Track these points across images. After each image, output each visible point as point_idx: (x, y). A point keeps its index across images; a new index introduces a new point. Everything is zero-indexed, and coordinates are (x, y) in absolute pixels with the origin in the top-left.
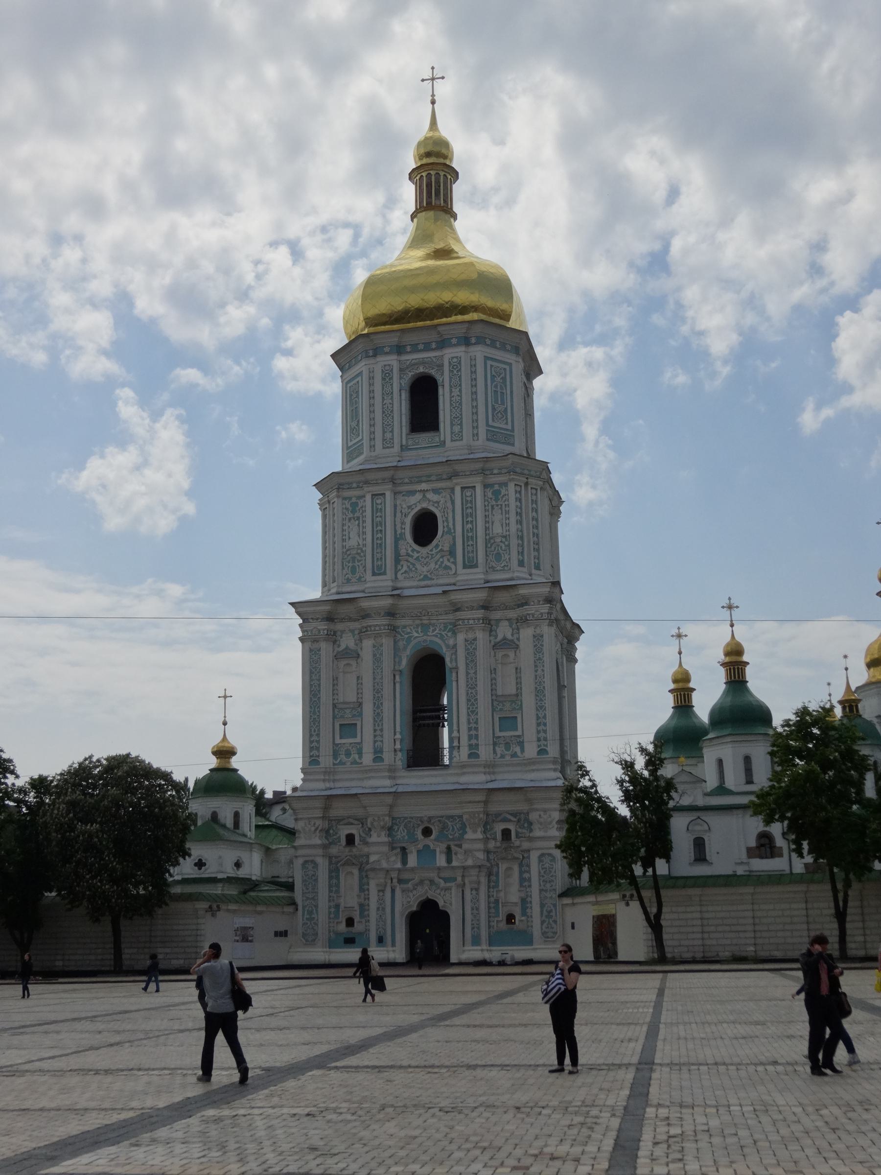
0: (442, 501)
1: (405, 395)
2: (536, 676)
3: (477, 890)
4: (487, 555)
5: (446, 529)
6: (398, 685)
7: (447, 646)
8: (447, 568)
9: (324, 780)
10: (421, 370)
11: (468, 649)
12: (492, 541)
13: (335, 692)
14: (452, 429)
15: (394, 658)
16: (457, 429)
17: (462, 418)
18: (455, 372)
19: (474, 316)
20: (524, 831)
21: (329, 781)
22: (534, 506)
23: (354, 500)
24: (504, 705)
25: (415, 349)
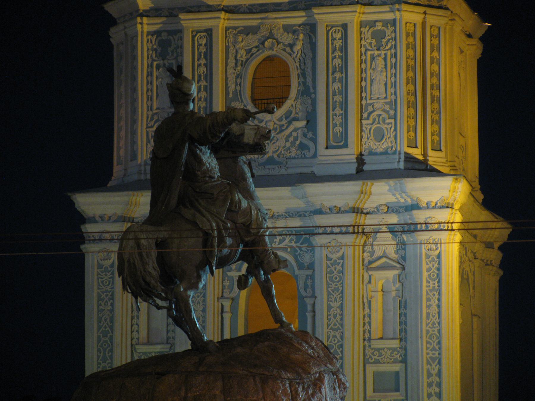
2: (428, 314)
4: (362, 131)
5: (302, 88)
7: (301, 266)
8: (302, 147)
11: (331, 272)
12: (370, 109)
13: (135, 327)
15: (223, 280)
22: (435, 54)
23: (164, 36)
24: (380, 355)
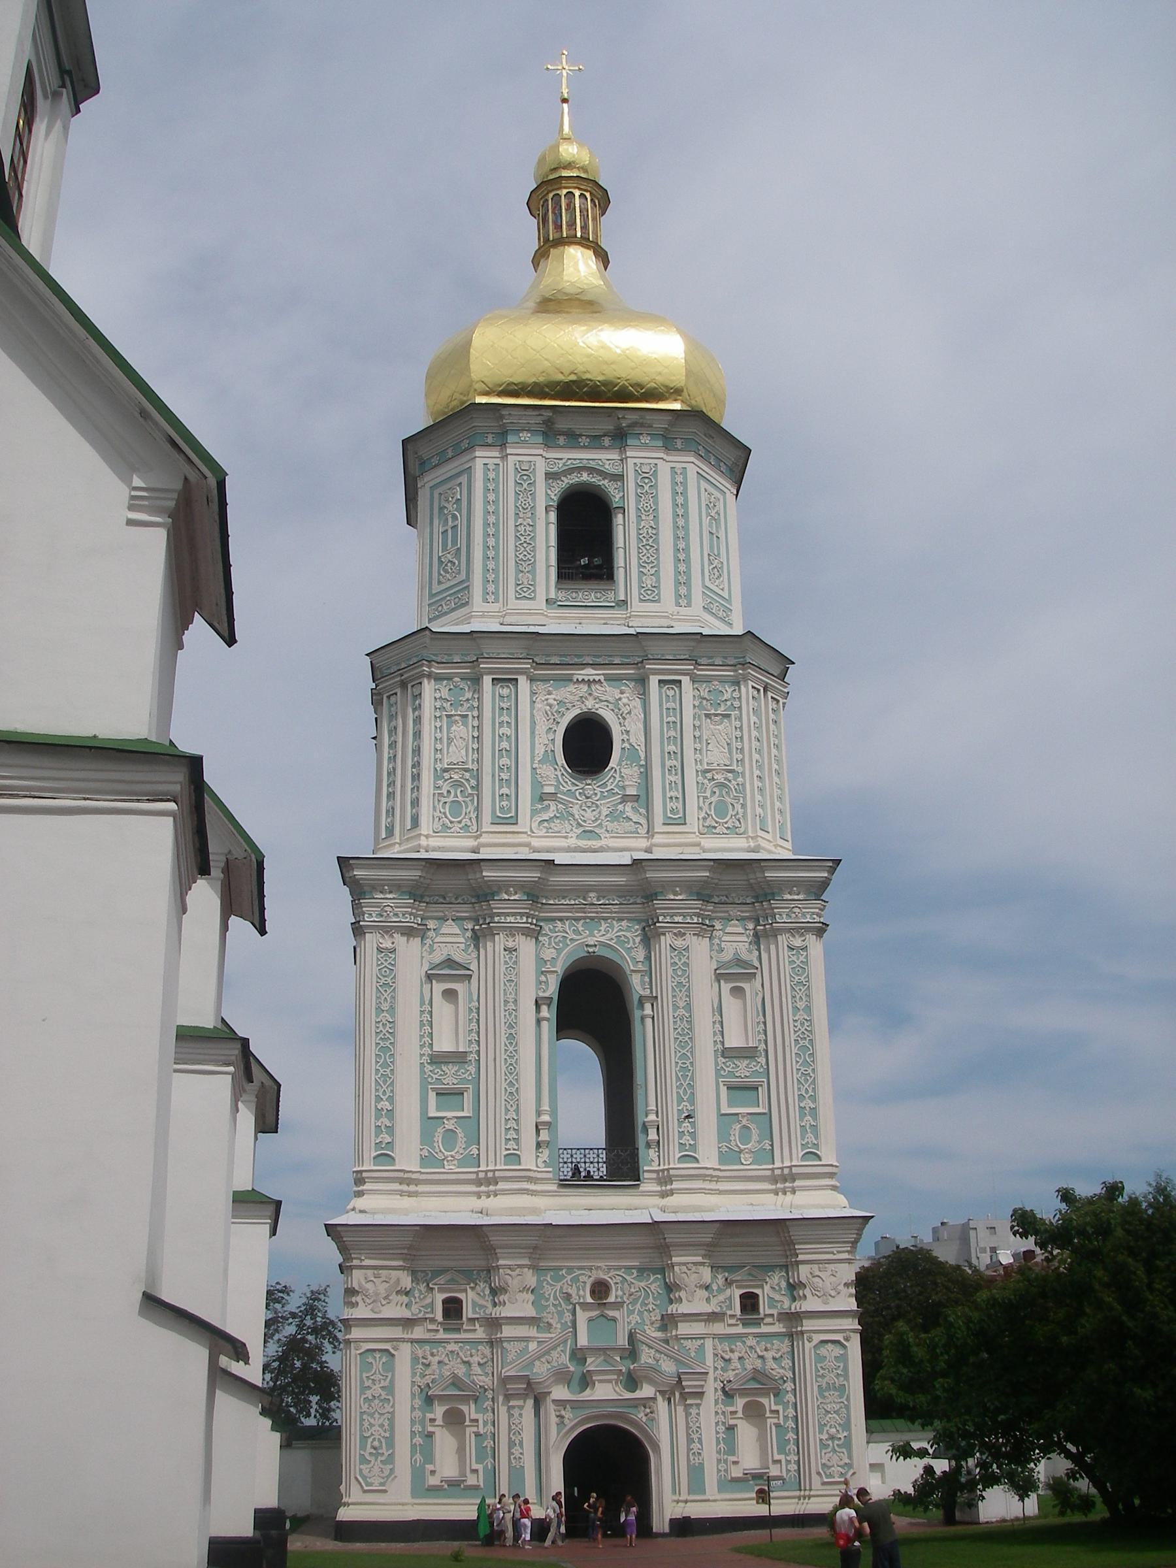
0: (625, 701)
1: (553, 516)
3: (698, 1405)
6: (545, 1024)
9: (401, 1193)
10: (585, 477)
14: (640, 581)
16: (649, 582)
17: (658, 566)
18: (646, 488)
19: (677, 406)
20: (782, 1298)
21: (410, 1194)
25: (573, 439)
